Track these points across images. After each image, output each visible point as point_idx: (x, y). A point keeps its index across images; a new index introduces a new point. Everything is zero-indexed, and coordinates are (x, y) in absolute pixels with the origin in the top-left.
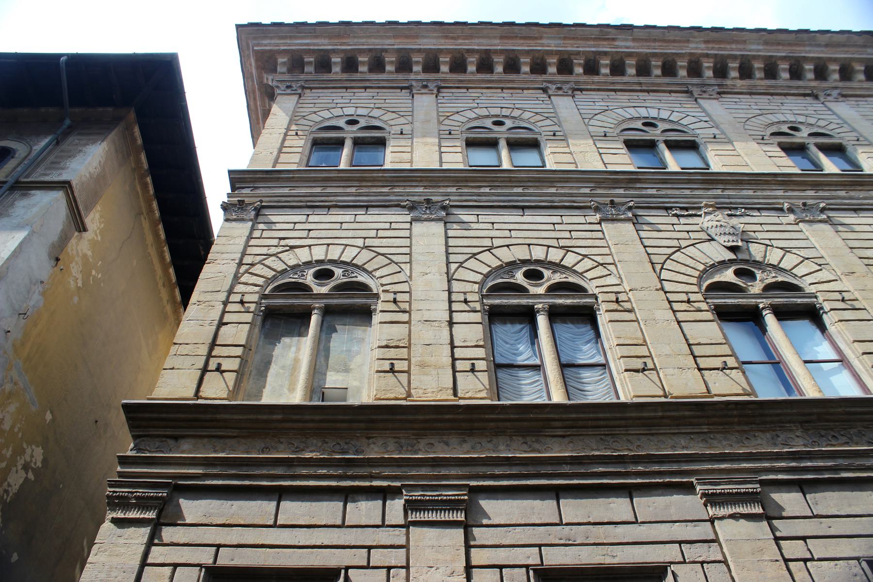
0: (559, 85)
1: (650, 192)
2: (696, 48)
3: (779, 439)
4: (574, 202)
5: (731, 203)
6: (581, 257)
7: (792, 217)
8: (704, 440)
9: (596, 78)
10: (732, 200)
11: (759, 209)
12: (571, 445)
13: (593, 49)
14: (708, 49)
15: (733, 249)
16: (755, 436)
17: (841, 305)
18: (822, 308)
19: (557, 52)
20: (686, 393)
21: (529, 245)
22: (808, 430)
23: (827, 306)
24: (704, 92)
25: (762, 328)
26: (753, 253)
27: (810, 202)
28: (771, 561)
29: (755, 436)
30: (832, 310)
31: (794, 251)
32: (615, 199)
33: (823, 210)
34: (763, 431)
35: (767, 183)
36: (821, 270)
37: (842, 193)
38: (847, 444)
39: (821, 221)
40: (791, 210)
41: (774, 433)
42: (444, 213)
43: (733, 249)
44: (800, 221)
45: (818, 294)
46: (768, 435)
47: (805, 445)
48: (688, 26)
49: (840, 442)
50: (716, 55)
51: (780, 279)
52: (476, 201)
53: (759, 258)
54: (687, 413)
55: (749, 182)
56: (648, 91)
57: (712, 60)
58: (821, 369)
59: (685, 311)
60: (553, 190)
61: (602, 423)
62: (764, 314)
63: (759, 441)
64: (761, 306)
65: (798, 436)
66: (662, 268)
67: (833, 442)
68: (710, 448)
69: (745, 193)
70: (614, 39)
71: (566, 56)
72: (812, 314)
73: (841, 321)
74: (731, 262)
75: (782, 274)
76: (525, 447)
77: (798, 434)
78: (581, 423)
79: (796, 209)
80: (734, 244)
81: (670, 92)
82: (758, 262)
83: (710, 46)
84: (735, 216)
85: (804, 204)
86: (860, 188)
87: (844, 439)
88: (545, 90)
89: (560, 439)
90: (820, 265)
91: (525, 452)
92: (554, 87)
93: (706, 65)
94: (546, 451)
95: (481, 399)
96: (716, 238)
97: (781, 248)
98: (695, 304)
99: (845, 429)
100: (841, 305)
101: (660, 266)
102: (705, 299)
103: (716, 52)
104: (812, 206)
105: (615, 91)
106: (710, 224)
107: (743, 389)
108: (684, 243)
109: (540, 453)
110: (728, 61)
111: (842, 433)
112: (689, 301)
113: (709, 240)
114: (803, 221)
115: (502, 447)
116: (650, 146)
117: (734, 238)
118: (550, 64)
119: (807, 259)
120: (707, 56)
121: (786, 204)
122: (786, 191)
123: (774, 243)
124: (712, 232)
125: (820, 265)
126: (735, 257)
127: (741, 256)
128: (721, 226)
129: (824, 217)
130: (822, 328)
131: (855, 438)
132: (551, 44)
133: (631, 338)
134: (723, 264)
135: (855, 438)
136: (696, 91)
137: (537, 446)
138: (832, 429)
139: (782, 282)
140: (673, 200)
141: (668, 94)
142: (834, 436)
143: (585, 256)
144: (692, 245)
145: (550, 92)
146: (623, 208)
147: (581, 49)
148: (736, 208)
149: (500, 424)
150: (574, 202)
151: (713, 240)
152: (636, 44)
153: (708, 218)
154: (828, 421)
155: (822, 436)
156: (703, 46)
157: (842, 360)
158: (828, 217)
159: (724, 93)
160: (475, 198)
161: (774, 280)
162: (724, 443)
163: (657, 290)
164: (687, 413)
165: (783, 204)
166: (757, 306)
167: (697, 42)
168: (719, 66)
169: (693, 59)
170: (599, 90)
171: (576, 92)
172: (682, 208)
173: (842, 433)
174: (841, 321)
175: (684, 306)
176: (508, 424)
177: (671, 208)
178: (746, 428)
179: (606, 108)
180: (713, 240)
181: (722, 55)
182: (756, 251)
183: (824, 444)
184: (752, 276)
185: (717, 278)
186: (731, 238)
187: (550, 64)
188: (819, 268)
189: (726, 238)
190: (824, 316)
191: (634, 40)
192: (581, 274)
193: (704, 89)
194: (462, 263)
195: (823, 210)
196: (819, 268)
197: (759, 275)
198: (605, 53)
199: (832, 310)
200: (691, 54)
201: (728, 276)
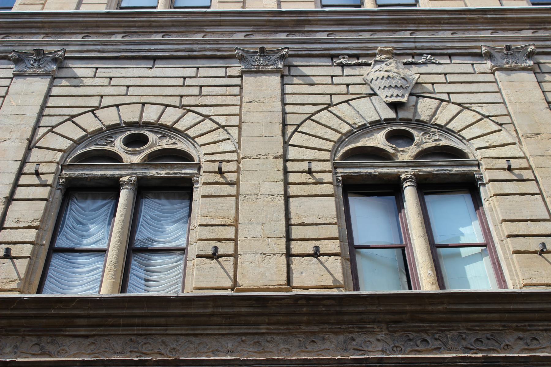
1: (319, 36)
3: (354, 343)
4: (218, 50)
5: (416, 48)
6: (201, 118)
7: (488, 65)
8: (258, 343)
10: (418, 45)
11: (450, 56)
12: (92, 347)
15: (395, 106)
16: (324, 339)
17: (507, 175)
18: (481, 179)
21: (117, 106)
22: (395, 332)
23: (487, 176)
25: (400, 205)
26: (419, 110)
27: (514, 45)
29: (324, 339)
30: (491, 181)
31: (474, 107)
32: (265, 46)
33: (530, 55)
34: (336, 333)
35: (472, 21)
36: (500, 130)
38: (438, 349)
39: (524, 69)
40: (489, 56)
41: (350, 335)
42: (54, 67)
43: (395, 106)
45: (482, 162)
46: (341, 338)
47: (383, 351)
49: (430, 347)
51: (444, 142)
52: (99, 51)
53: (424, 116)
54: (244, 310)
55: (449, 22)
58: (459, 255)
59: (303, 183)
60: (199, 37)
61: (136, 321)
62: (405, 185)
63: (327, 345)
64: (403, 176)
65: (378, 340)
66: (296, 131)
67: (421, 348)
68: (263, 352)
69: (441, 35)
72: (469, 186)
73: (496, 195)
74: (388, 121)
75: (448, 136)
76: (36, 349)
77: (379, 337)
78: (110, 321)
79: (496, 55)
80: (398, 99)
82: (422, 121)
84: (416, 64)
85: (508, 48)
87: (437, 344)
89: (81, 340)
90: (501, 125)
91: (34, 355)
94: (59, 354)
95: (9, 291)
96: (378, 92)
97: (459, 104)
98: (317, 176)
99: (443, 331)
100: (507, 175)
101: (294, 128)
102: (335, 168)
104: (518, 50)
106: (373, 75)
107: (335, 280)
108: (336, 99)
109: (51, 356)
111: (437, 336)
112: (310, 172)
113: (370, 95)
114: (501, 69)
115: (7, 350)
117: (400, 93)
119: (488, 117)
121: (483, 48)
122: (495, 31)
123: (453, 98)
124: (375, 85)
125: (501, 125)
126: (393, 116)
127: (402, 114)
128: (389, 77)
129: (530, 63)
130: (477, 203)
131: (450, 342)
133: (219, 217)
134: (377, 125)
135: (450, 342)
137: (50, 348)
138: (426, 331)
139: (445, 147)
140: (341, 46)
142: (425, 340)
143: (207, 117)
144: (347, 101)
146: (274, 57)
148: (421, 55)
149: (14, 321)
150: (218, 50)
151: (375, 94)
153: (377, 67)
154: (423, 321)
155: (410, 340)
157: (487, 245)
158: (538, 64)
160: (99, 47)
161: (434, 144)
162: (282, 346)
163: (276, 158)
164: (244, 310)
165: (480, 48)
166: (398, 177)
172: (351, 56)
173: (437, 336)
174: (496, 195)
175: (303, 178)
176: (23, 321)
177: (337, 56)
178: (316, 329)
180: (375, 94)
182: (425, 108)
183: (408, 350)
184: (408, 138)
185: (364, 142)
186: (396, 92)
188: (498, 128)
189: (389, 92)
190: (482, 189)
192: (193, 139)
194: (53, 127)
195: (530, 55)
196: (498, 128)
197: (418, 135)
199: (491, 181)
201: (379, 140)
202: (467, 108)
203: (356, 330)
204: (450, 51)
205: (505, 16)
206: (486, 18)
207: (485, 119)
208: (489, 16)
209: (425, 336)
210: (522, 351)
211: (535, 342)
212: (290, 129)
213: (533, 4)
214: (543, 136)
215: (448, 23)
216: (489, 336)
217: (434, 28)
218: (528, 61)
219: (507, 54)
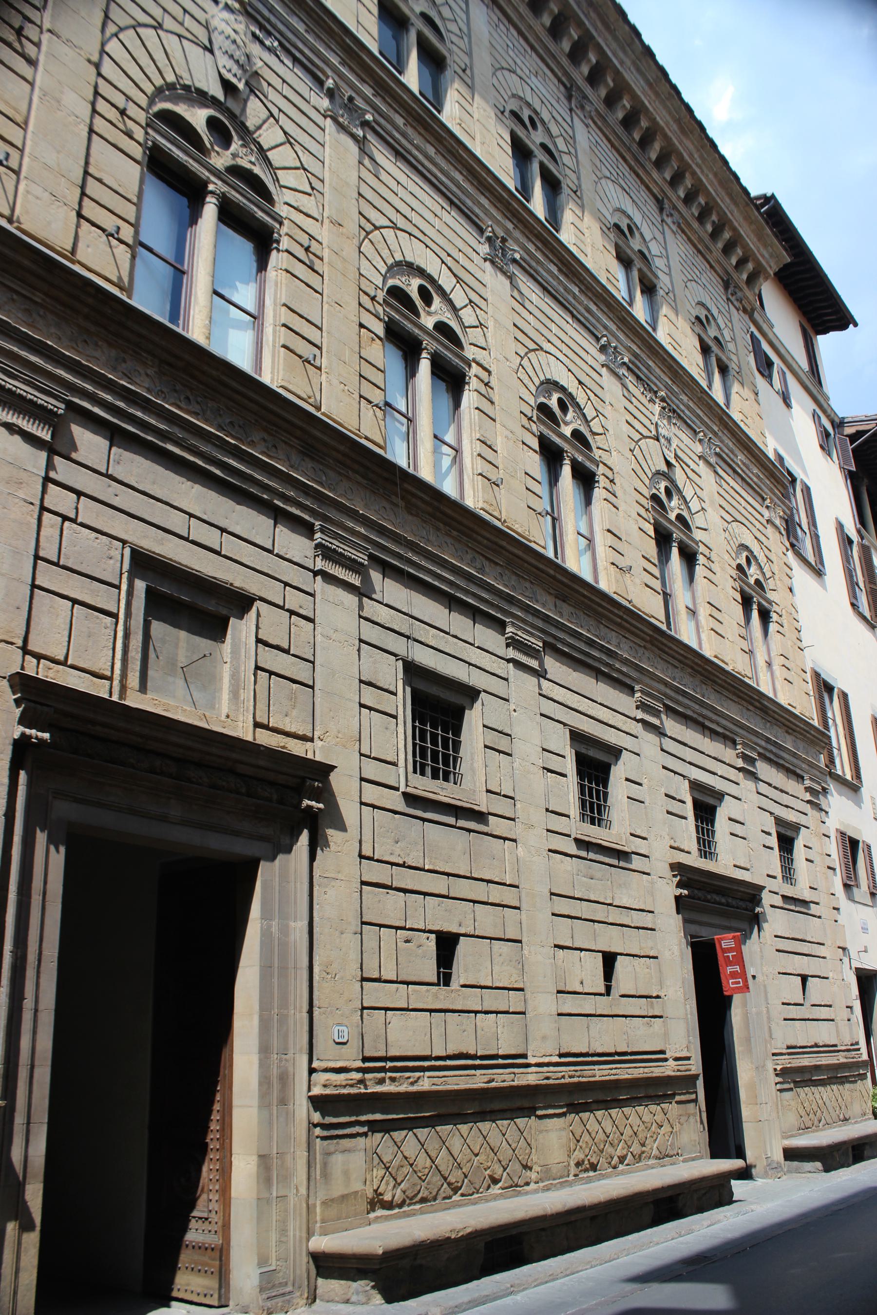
3: (124, 365)
5: (268, 21)
7: (325, 103)
8: (27, 311)
10: (273, 19)
11: (295, 60)
15: (228, 87)
17: (301, 253)
18: (278, 242)
20: (40, 235)
23: (285, 243)
25: (194, 216)
26: (248, 111)
27: (359, 102)
28: (25, 501)
29: (96, 345)
30: (287, 251)
31: (297, 148)
33: (365, 124)
34: (110, 345)
35: (330, 32)
36: (310, 195)
37: (400, 121)
38: (195, 414)
39: (353, 136)
40: (331, 94)
43: (228, 87)
44: (331, 117)
45: (286, 222)
46: (113, 353)
47: (149, 391)
49: (190, 408)
51: (257, 170)
53: (250, 123)
54: (26, 262)
58: (228, 312)
62: (208, 199)
63: (97, 354)
64: (211, 187)
65: (147, 375)
66: (116, 35)
67: (183, 405)
68: (30, 326)
72: (262, 241)
73: (287, 271)
74: (213, 102)
75: (264, 165)
77: (149, 372)
79: (337, 97)
80: (234, 80)
82: (247, 128)
84: (262, 43)
85: (351, 99)
86: (422, 131)
87: (197, 408)
90: (313, 189)
96: (217, 52)
97: (285, 133)
98: (130, 123)
99: (205, 397)
100: (301, 253)
102: (148, 125)
106: (222, 26)
107: (120, 278)
108: (169, 23)
111: (199, 399)
113: (205, 48)
114: (335, 119)
117: (239, 73)
119: (305, 169)
121: (330, 81)
123: (283, 119)
124: (218, 41)
125: (313, 189)
126: (221, 97)
127: (231, 104)
128: (234, 42)
129: (360, 133)
130: (262, 265)
131: (209, 412)
134: (202, 98)
135: (209, 412)
139: (257, 177)
142: (188, 398)
144: (179, 36)
148: (269, 34)
151: (211, 51)
153: (226, 15)
155: (175, 391)
157: (256, 318)
158: (365, 137)
161: (248, 166)
162: (53, 330)
163: (89, 61)
164: (26, 262)
165: (327, 77)
166: (205, 183)
173: (199, 399)
174: (287, 271)
175: (113, 115)
180: (211, 51)
182: (254, 113)
183: (172, 400)
185: (181, 109)
186: (235, 69)
188: (309, 190)
189: (230, 64)
190: (274, 253)
195: (365, 124)
196: (309, 190)
197: (236, 145)
199: (287, 251)
201: (198, 117)
202: (291, 144)
203: (131, 352)
204: (298, 55)
205: (361, 53)
206: (344, 41)
207: (302, 171)
208: (348, 41)
209: (189, 394)
210: (262, 453)
211: (274, 450)
212: (111, 29)
213: (381, 53)
214: (345, 230)
215: (307, 13)
216: (241, 423)
217: (292, 6)
218: (359, 129)
219: (346, 105)
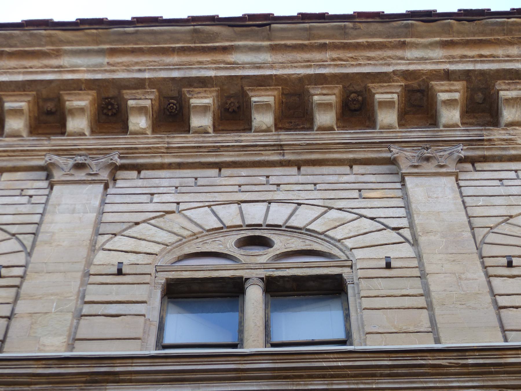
0: (80, 160)
2: (423, 60)
9: (178, 140)
13: (176, 74)
14: (451, 60)
19: (91, 84)
24: (428, 159)
48: (402, 10)
50: (468, 72)
56: (298, 165)
57: (459, 85)
70: (225, 50)
71: (112, 93)
81: (352, 163)
83: (458, 52)
88: (47, 170)
92: (71, 162)
93: (443, 96)
103: (470, 67)
105: (219, 166)
110: (499, 85)
116: (228, 292)
118: (73, 112)
120: (448, 75)
132: (82, 66)
136: (406, 157)
141: (346, 169)
145: (57, 175)
147: (147, 75)
152: (280, 57)
156: (438, 53)
159: (485, 159)
167: (426, 46)
168: (479, 97)
169: (414, 84)
170: (180, 166)
171: (121, 174)
179: (173, 207)
181: (482, 73)
187: (73, 112)
191: (274, 49)
193: (427, 153)
198: (203, 83)
200: (406, 75)
